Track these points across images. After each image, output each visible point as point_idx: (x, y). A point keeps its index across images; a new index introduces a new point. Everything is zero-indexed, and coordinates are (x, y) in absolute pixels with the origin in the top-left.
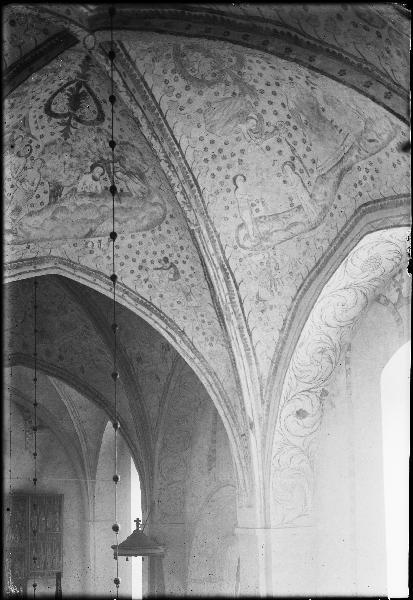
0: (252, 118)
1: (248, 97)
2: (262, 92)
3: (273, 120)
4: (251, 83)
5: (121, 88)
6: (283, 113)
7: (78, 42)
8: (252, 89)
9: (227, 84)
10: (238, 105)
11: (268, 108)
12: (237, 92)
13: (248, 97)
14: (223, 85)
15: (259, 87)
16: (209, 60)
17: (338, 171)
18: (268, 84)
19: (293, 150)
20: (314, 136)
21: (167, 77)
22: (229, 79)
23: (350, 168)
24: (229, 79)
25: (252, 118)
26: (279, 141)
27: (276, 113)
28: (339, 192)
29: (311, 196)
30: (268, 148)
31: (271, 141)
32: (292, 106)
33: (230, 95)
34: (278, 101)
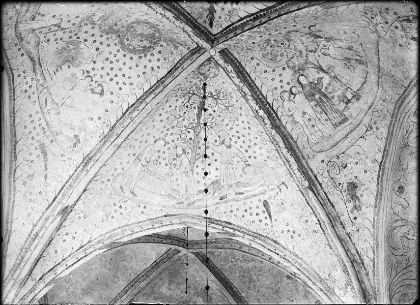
0: (98, 21)
1: (107, 28)
2: (101, 36)
3: (85, 28)
4: (109, 36)
5: (191, 34)
6: (83, 36)
7: (219, 52)
8: (107, 34)
9: (123, 27)
10: (110, 22)
11: (93, 31)
12: (115, 27)
13: (107, 28)
14: (125, 25)
15: (105, 36)
16: (139, 33)
17: (36, 59)
18: (101, 43)
19: (63, 29)
20: (60, 48)
21: (161, 24)
22: (123, 30)
23: (34, 70)
24: (123, 30)
25: (98, 21)
26: (74, 24)
27: (86, 32)
28: (25, 56)
29: (34, 30)
30: (77, 17)
31: (78, 21)
32: (82, 46)
33: (118, 23)
34: (91, 39)
